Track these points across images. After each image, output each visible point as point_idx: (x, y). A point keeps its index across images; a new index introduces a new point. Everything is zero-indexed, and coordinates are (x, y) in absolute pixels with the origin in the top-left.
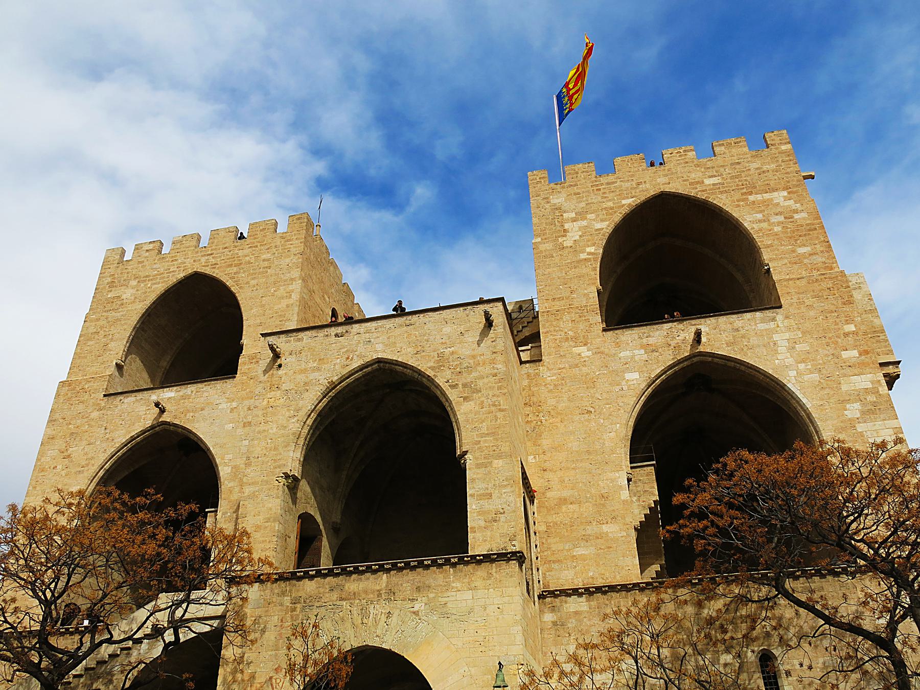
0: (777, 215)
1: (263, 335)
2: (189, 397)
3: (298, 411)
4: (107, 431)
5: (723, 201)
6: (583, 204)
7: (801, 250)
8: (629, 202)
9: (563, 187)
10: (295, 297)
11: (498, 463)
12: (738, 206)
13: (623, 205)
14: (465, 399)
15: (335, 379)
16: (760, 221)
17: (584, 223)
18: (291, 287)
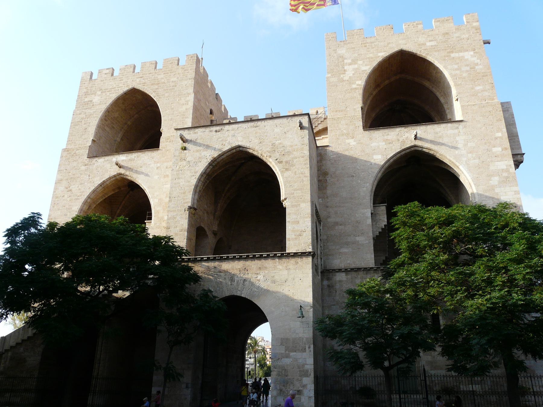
0: (466, 66)
1: (177, 129)
2: (134, 160)
3: (196, 172)
4: (91, 177)
7: (478, 88)
8: (383, 54)
9: (345, 44)
10: (191, 104)
11: (303, 205)
12: (445, 60)
13: (379, 56)
14: (287, 170)
16: (456, 69)
17: (356, 66)
18: (188, 99)
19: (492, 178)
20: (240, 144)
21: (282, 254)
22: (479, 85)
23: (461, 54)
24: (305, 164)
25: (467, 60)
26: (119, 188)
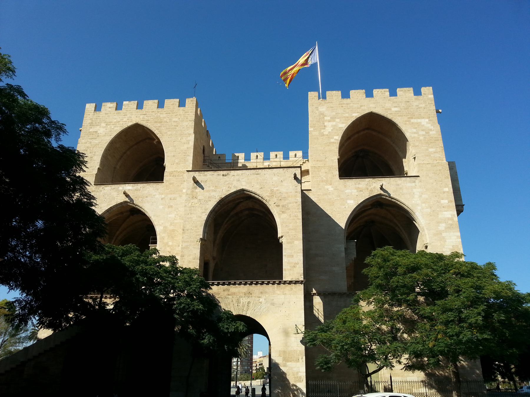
0: (422, 130)
3: (206, 210)
5: (399, 121)
6: (334, 113)
7: (431, 150)
8: (356, 115)
12: (406, 124)
14: (283, 212)
15: (223, 196)
16: (415, 133)
17: (334, 123)
21: (280, 282)
22: (432, 147)
23: (419, 120)
24: (298, 209)
26: (122, 213)
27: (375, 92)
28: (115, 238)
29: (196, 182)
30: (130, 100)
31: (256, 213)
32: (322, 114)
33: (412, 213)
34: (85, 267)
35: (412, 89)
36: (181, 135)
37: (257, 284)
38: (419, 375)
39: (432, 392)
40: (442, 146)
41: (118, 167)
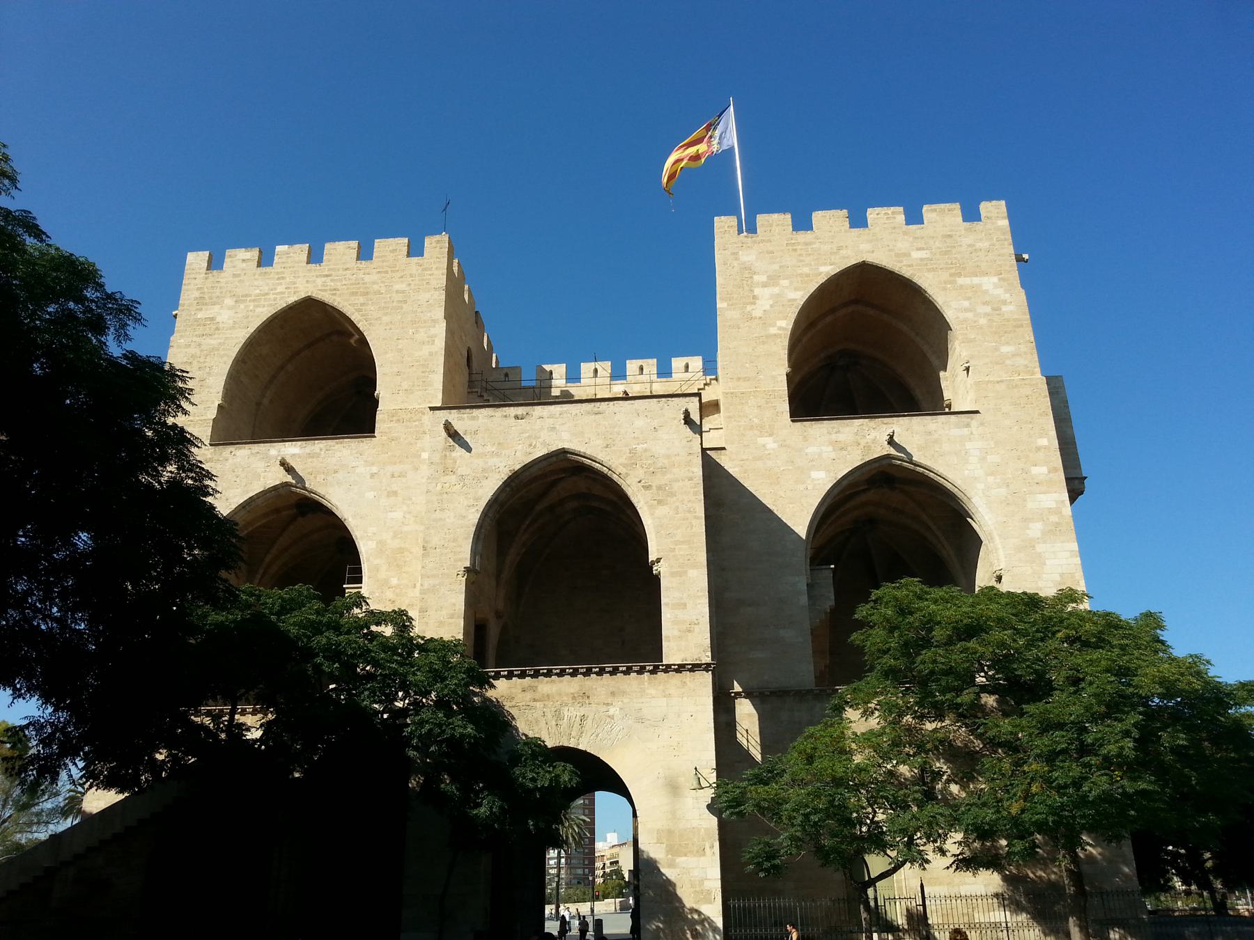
2: (318, 455)
5: (928, 282)
6: (776, 267)
7: (1005, 349)
8: (828, 270)
9: (755, 242)
10: (440, 343)
14: (660, 502)
15: (517, 467)
16: (966, 310)
17: (776, 290)
18: (433, 331)
19: (1031, 525)
20: (566, 446)
22: (1008, 343)
23: (976, 280)
25: (986, 292)
27: (872, 214)
28: (261, 571)
29: (453, 434)
30: (291, 242)
31: (595, 504)
32: (748, 269)
33: (965, 499)
34: (192, 641)
35: (957, 206)
36: (413, 322)
37: (601, 673)
38: (988, 881)
39: (1019, 918)
40: (1032, 339)
41: (266, 401)
